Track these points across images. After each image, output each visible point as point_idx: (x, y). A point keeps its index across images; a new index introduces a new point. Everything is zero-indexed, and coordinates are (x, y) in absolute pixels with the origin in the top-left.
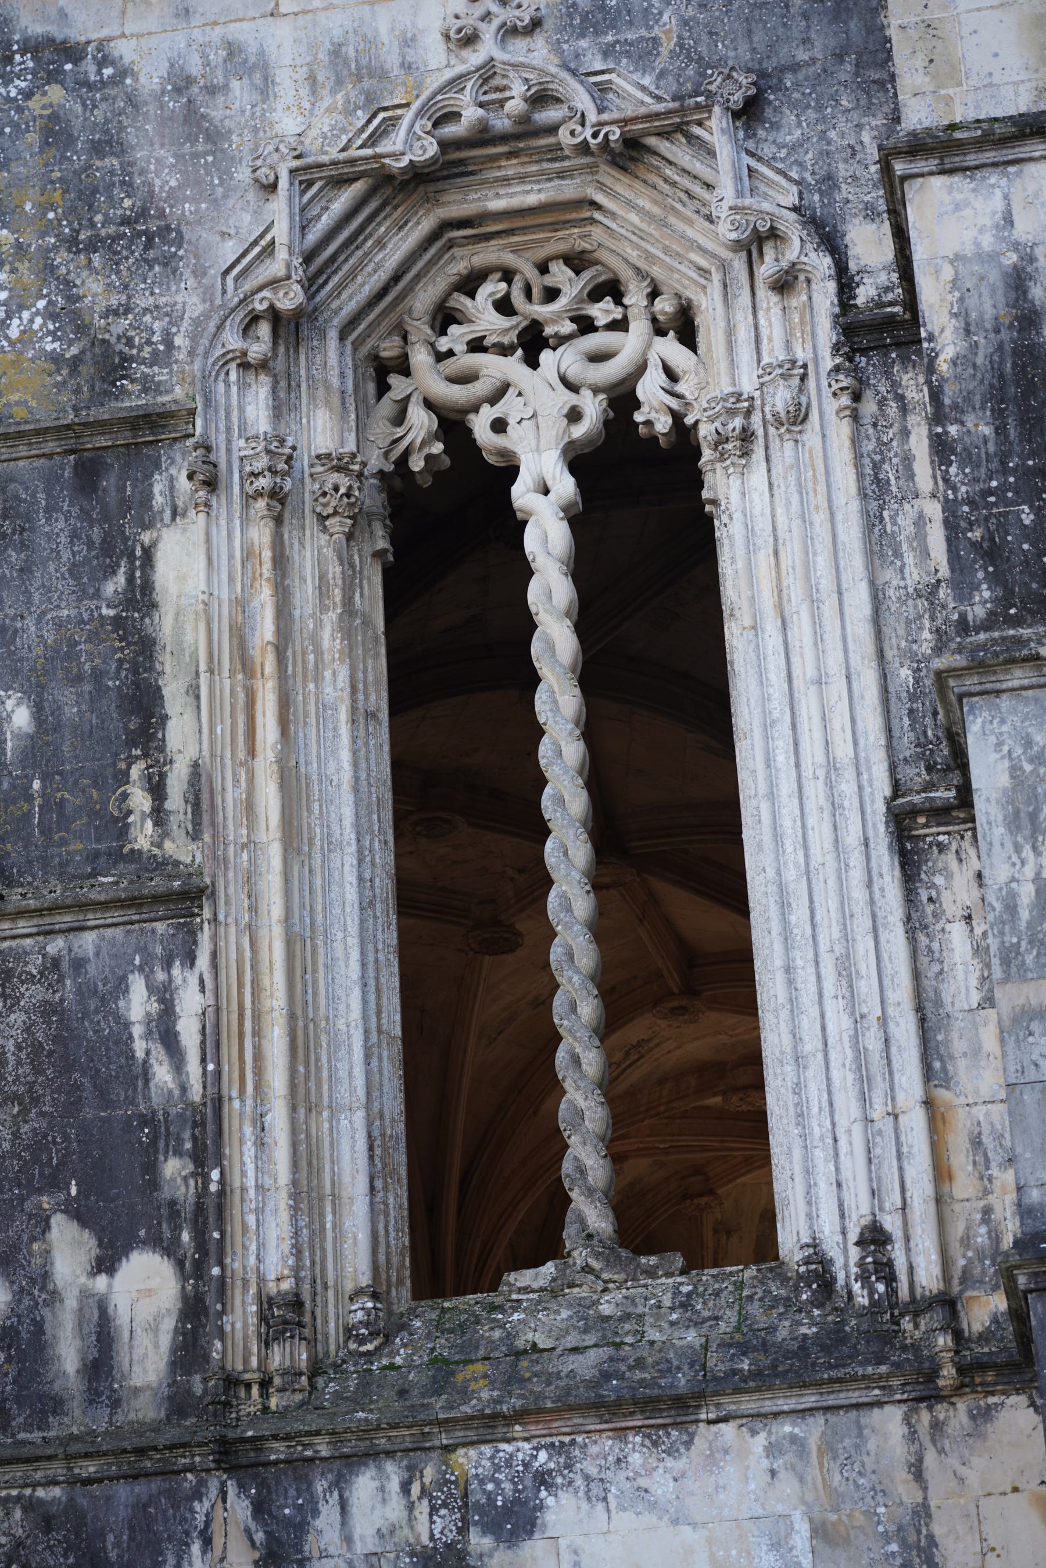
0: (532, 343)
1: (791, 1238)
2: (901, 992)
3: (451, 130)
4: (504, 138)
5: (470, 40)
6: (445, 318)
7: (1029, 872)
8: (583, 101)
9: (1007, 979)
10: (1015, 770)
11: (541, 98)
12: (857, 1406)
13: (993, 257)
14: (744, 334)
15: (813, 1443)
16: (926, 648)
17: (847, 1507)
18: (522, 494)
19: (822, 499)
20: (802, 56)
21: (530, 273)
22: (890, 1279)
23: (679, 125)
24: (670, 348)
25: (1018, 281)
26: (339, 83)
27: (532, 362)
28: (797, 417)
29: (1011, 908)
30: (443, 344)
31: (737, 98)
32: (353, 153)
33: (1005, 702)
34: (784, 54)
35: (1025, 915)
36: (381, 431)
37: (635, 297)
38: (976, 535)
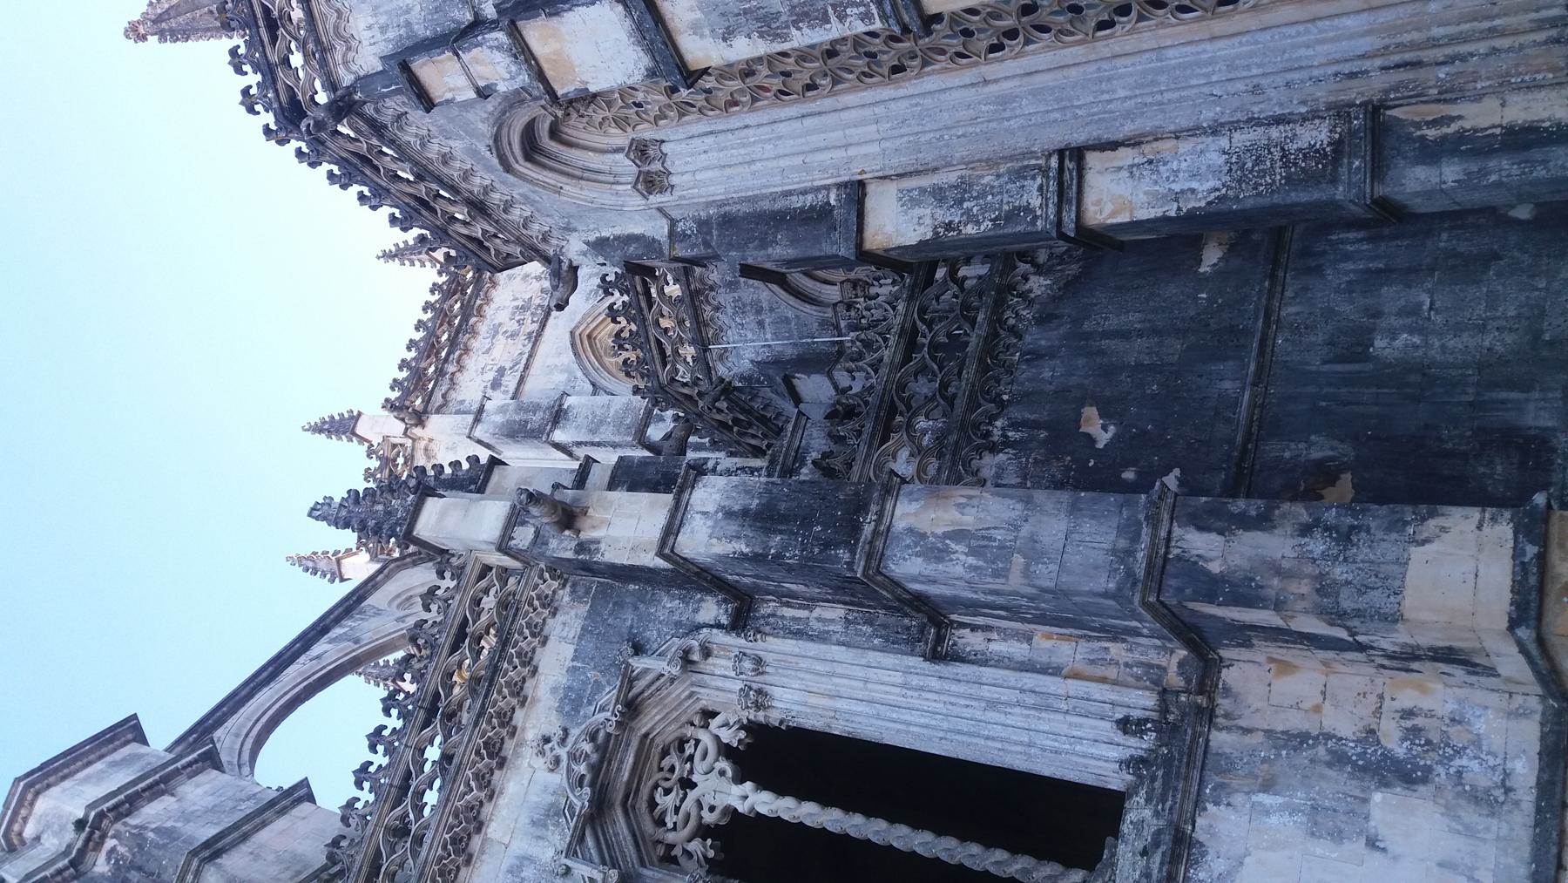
0: (687, 784)
1: (1116, 781)
2: (1012, 677)
3: (587, 781)
4: (601, 762)
5: (557, 761)
6: (660, 822)
7: (963, 557)
8: (601, 717)
9: (1006, 577)
10: (917, 555)
11: (593, 737)
12: (1205, 752)
13: (716, 522)
14: (720, 683)
15: (1218, 779)
16: (870, 630)
17: (1256, 771)
18: (742, 808)
19: (794, 660)
20: (629, 623)
21: (661, 775)
22: (1147, 720)
23: (630, 679)
24: (714, 723)
25: (729, 514)
26: (545, 826)
27: (693, 785)
28: (759, 661)
29: (975, 568)
30: (670, 825)
31: (630, 651)
32: (572, 825)
33: (888, 553)
34: (624, 630)
35: (981, 563)
36: (690, 865)
37: (689, 731)
38: (816, 550)
